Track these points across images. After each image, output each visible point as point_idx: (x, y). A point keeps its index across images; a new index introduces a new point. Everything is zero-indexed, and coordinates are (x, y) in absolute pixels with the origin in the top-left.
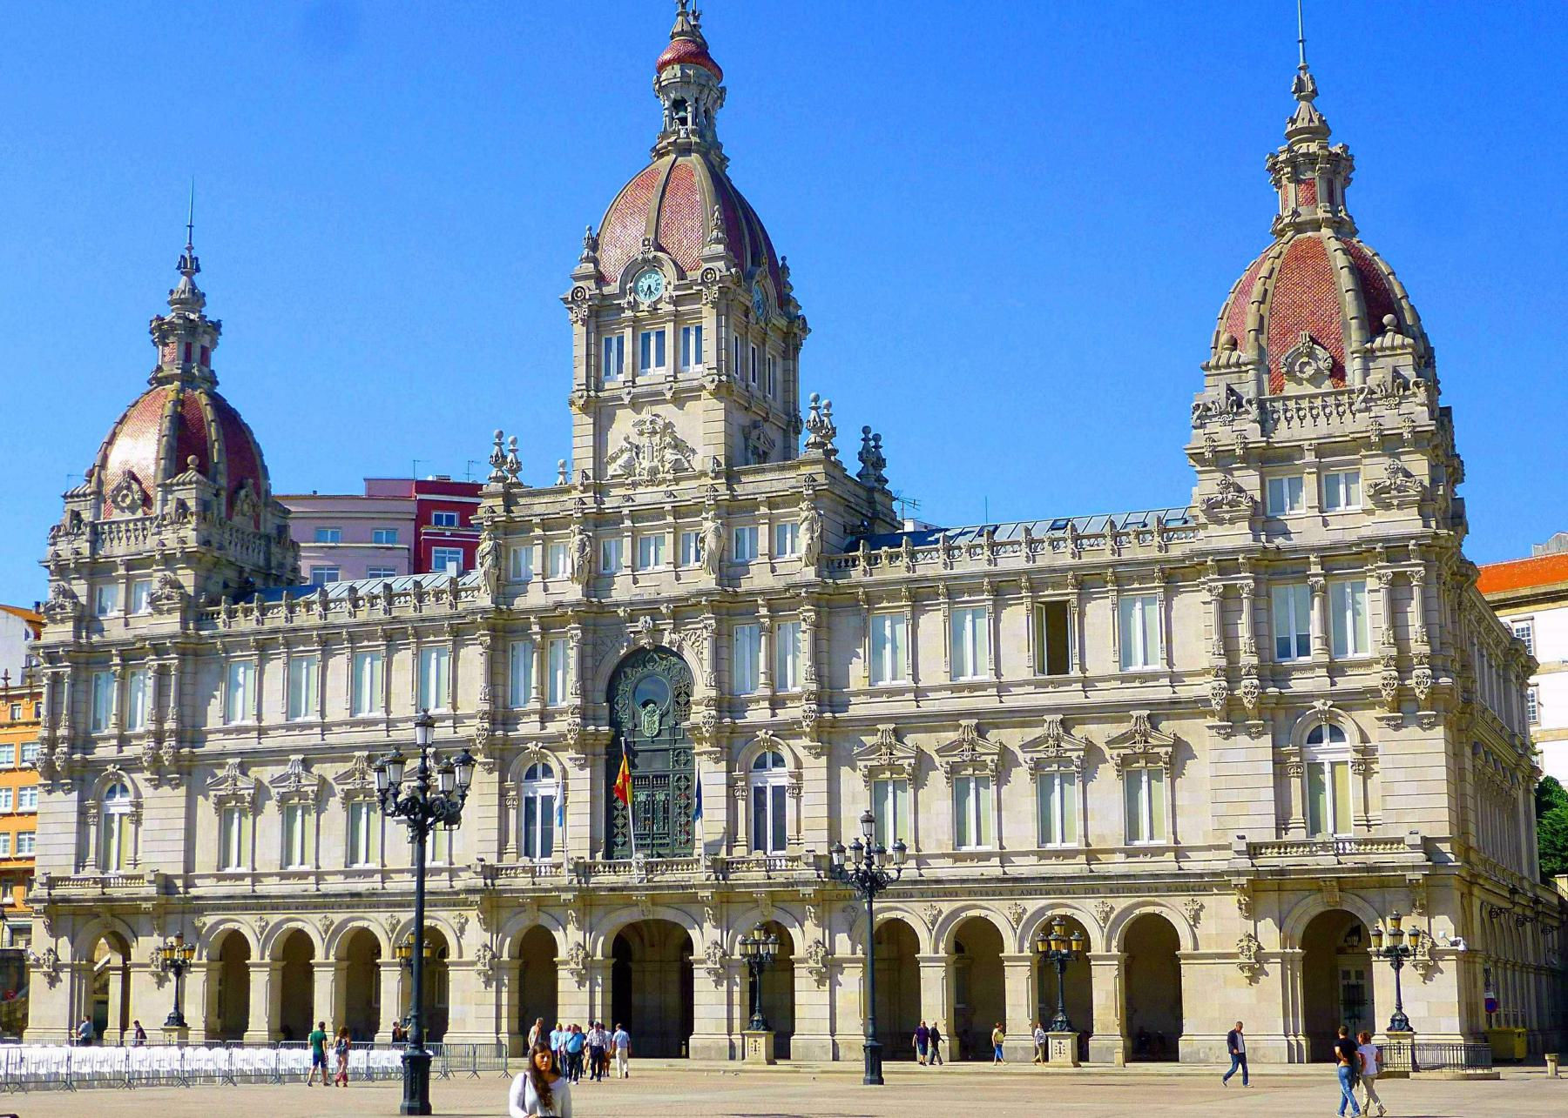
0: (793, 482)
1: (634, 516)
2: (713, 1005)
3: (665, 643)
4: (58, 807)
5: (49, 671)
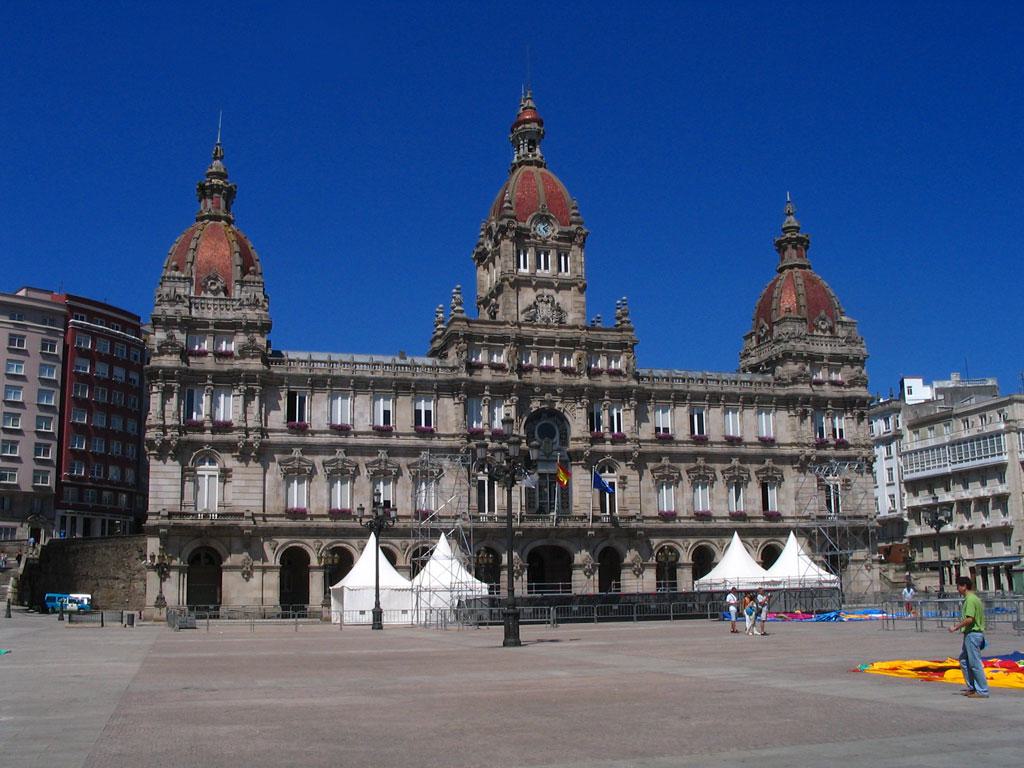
0: (619, 338)
1: (539, 342)
3: (556, 408)
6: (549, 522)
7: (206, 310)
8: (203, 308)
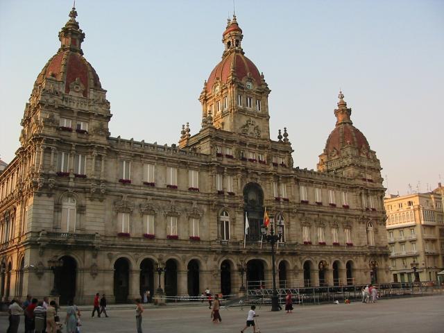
4: (46, 203)
5: (45, 146)
7: (72, 103)
8: (70, 102)
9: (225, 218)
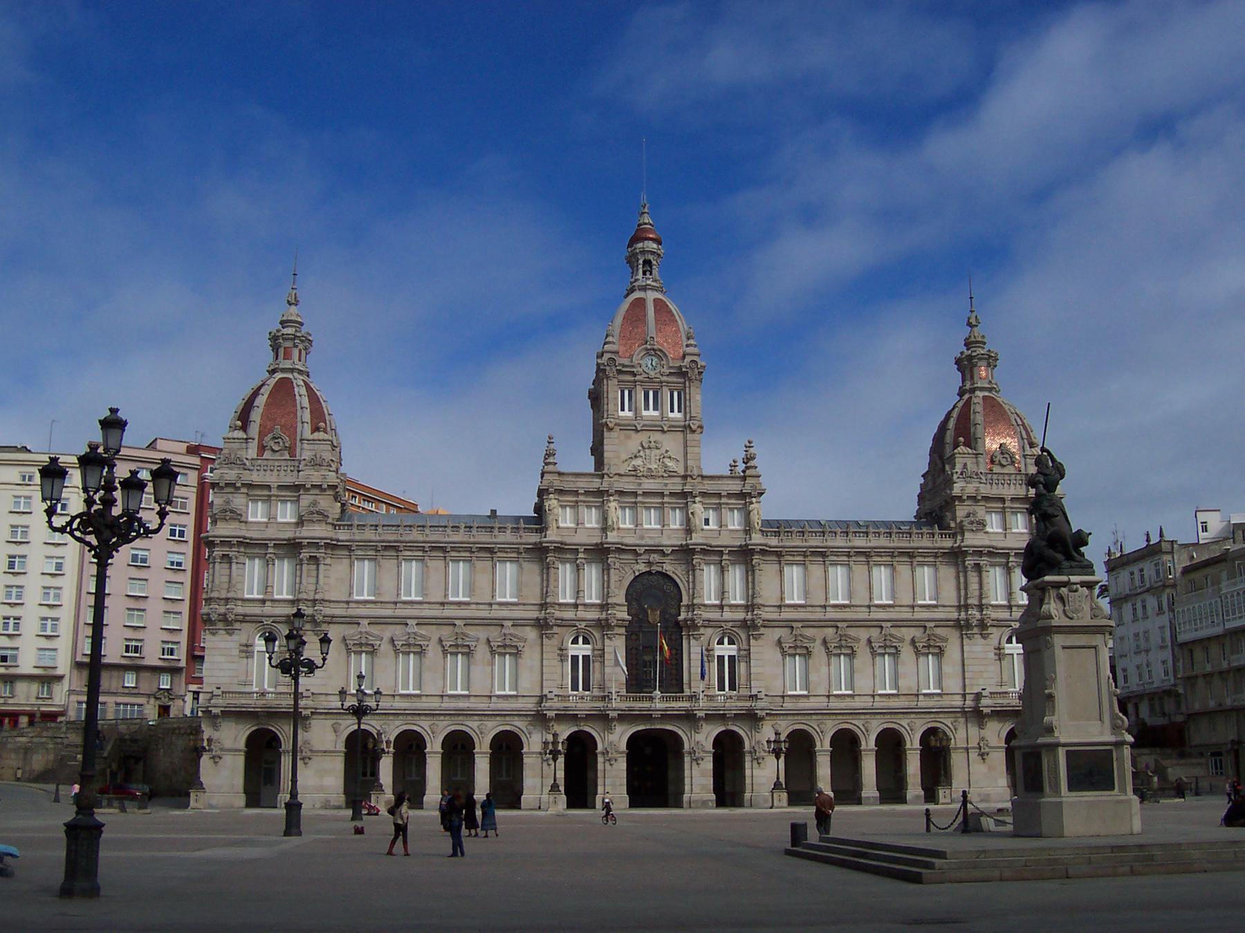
2: (698, 778)
4: (222, 645)
6: (659, 702)
9: (582, 650)
